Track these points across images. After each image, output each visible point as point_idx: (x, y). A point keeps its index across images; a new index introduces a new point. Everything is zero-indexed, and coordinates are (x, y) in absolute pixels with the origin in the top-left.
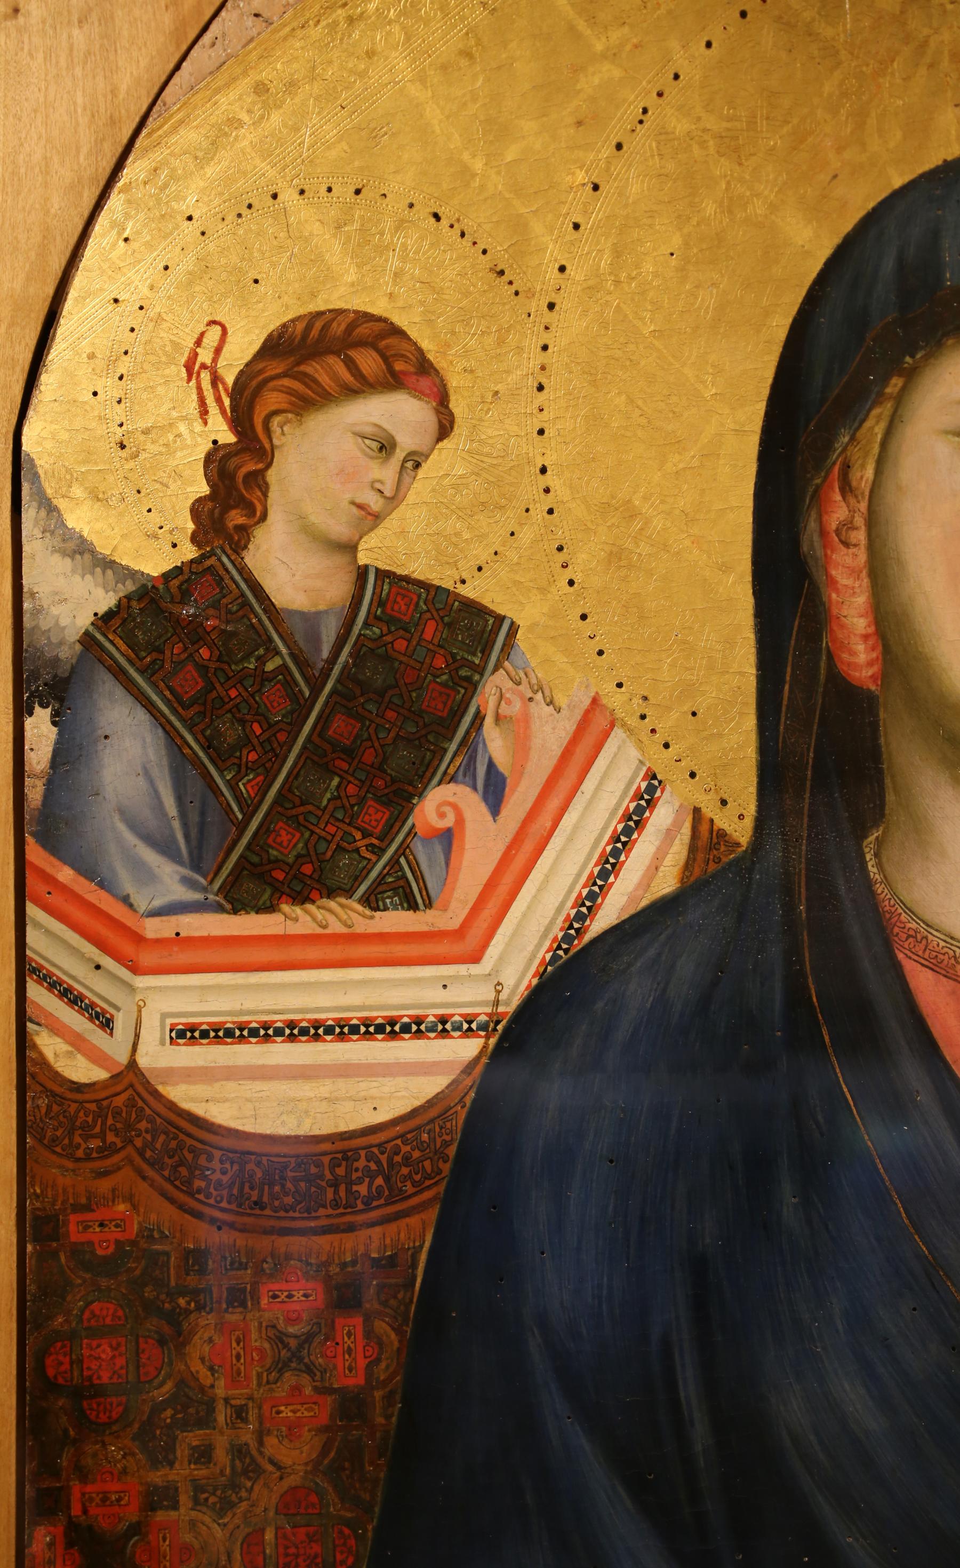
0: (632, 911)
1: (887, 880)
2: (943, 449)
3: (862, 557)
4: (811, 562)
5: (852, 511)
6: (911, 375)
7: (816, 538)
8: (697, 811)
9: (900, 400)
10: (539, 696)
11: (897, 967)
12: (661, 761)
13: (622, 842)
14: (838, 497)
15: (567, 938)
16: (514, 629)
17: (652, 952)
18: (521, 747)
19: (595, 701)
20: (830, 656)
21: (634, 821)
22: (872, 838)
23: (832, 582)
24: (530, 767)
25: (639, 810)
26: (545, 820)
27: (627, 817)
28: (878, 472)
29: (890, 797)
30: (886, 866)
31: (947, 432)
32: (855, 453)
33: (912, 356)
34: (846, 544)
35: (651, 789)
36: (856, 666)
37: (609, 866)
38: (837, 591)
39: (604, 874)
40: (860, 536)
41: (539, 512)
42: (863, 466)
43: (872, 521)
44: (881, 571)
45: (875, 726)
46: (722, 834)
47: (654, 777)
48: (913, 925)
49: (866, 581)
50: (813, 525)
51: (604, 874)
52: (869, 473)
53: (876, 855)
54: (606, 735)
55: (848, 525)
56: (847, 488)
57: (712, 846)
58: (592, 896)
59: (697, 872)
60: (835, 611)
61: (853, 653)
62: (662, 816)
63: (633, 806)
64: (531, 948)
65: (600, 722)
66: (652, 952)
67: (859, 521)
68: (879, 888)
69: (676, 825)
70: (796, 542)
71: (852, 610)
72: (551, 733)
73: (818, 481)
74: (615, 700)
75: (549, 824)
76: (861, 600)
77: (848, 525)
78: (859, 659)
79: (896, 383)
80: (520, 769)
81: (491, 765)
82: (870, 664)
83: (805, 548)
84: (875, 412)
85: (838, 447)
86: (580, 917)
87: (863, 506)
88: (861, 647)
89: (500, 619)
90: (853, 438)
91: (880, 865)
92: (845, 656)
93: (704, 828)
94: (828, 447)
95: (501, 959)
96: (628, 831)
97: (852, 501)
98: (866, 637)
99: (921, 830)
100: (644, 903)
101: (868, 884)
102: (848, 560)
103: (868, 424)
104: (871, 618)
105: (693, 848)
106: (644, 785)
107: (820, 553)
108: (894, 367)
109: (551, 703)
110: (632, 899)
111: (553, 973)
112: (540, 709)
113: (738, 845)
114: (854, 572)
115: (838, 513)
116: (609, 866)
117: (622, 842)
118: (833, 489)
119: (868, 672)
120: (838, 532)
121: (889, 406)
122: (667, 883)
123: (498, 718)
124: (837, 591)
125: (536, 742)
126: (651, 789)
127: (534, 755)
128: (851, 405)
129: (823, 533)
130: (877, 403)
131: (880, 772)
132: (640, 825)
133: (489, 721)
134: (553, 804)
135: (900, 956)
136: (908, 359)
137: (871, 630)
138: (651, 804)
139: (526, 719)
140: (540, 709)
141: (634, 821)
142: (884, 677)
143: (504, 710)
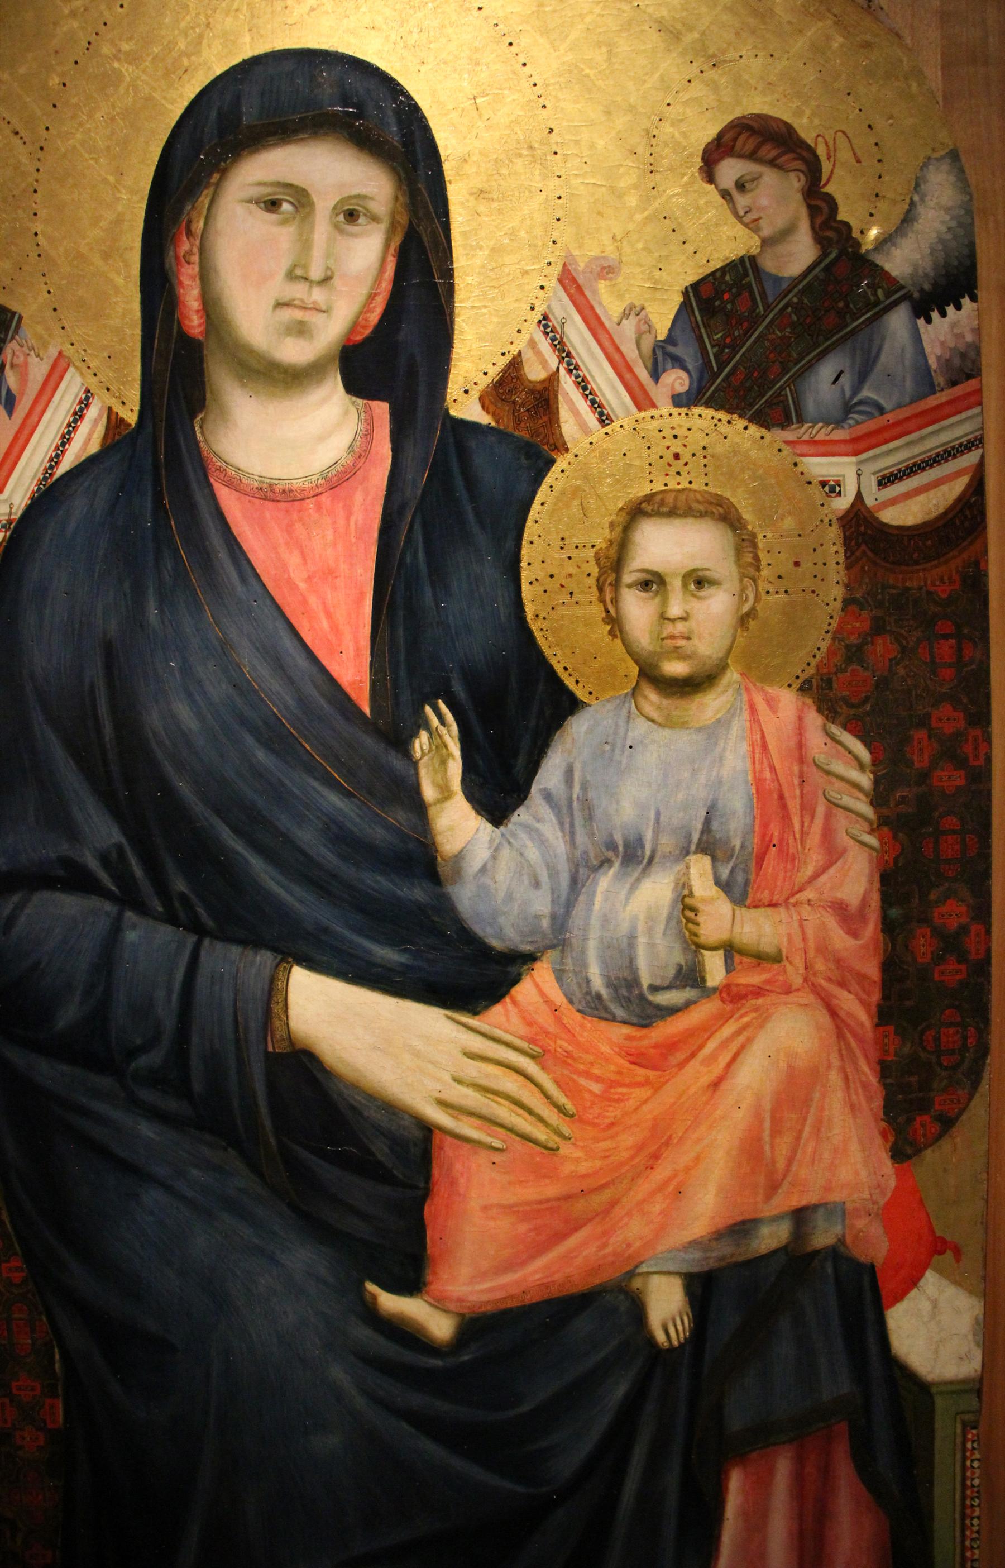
0: (77, 463)
1: (206, 441)
2: (240, 210)
3: (197, 269)
4: (170, 274)
5: (192, 245)
6: (224, 172)
7: (173, 260)
8: (110, 409)
9: (218, 185)
10: (32, 353)
11: (210, 486)
12: (92, 383)
13: (72, 427)
14: (185, 238)
15: (45, 479)
16: (20, 318)
17: (86, 484)
18: (23, 379)
19: (60, 353)
20: (179, 322)
21: (78, 415)
22: (198, 418)
23: (181, 283)
24: (28, 391)
25: (81, 410)
26: (34, 418)
27: (75, 413)
28: (206, 224)
29: (208, 395)
30: (206, 433)
31: (243, 201)
32: (194, 214)
33: (225, 162)
34: (189, 263)
35: (87, 398)
36: (193, 327)
37: (65, 440)
38: (183, 288)
39: (63, 444)
40: (195, 258)
41: (33, 255)
42: (198, 221)
43: (202, 250)
44: (206, 276)
45: (201, 360)
46: (122, 420)
47: (89, 391)
48: (219, 464)
49: (198, 282)
50: (171, 253)
51: (63, 444)
52: (201, 224)
53: (201, 427)
54: (65, 371)
55: (190, 253)
56: (189, 233)
57: (118, 426)
58: (57, 456)
59: (109, 441)
60: (182, 299)
61: (191, 320)
62: (92, 412)
63: (78, 408)
64: (27, 484)
65: (63, 364)
66: (86, 484)
67: (195, 250)
68: (202, 445)
69: (100, 416)
70: (162, 264)
71: (191, 297)
72: (38, 370)
73: (174, 231)
74: (69, 351)
75: (36, 419)
76: (196, 292)
77: (190, 253)
78: (194, 323)
79: (216, 177)
80: (23, 394)
81: (9, 390)
82: (200, 325)
83: (167, 266)
84: (205, 192)
85: (186, 212)
86: (51, 467)
87: (198, 242)
88: (195, 317)
89: (14, 313)
90: (193, 207)
91: (202, 433)
92: (187, 322)
93: (113, 417)
94: (180, 212)
95: (13, 491)
96: (75, 421)
97: (192, 239)
98: (198, 311)
99: (224, 413)
100: (83, 458)
101: (197, 443)
102: (190, 271)
103: (201, 199)
104: (200, 302)
105: (108, 428)
106: (84, 396)
107: (175, 268)
108: (215, 168)
109: (38, 356)
110: (77, 457)
111: (38, 497)
112: (33, 360)
113: (130, 425)
114: (192, 278)
115: (185, 246)
116: (65, 440)
117: (72, 427)
118: (181, 233)
119: (198, 330)
120: (184, 256)
121: (212, 189)
122: (94, 448)
123: (12, 366)
124: (183, 288)
125: (31, 377)
126: (87, 398)
127: (30, 384)
128: (192, 189)
129: (177, 258)
130: (206, 188)
131: (203, 383)
132: (81, 417)
133: (8, 367)
134: (39, 408)
135: (212, 480)
136: (223, 164)
137: (201, 308)
138: (87, 406)
139: (26, 364)
140: (33, 360)
141: (78, 415)
142: (207, 333)
143: (16, 361)
